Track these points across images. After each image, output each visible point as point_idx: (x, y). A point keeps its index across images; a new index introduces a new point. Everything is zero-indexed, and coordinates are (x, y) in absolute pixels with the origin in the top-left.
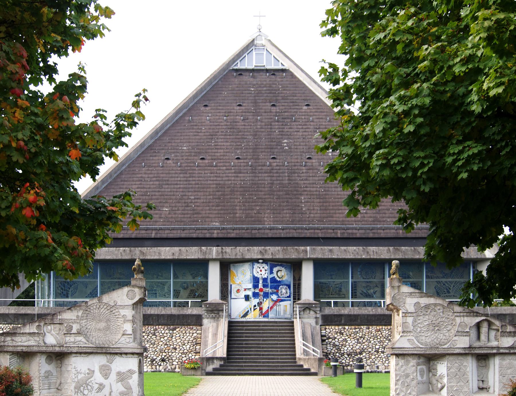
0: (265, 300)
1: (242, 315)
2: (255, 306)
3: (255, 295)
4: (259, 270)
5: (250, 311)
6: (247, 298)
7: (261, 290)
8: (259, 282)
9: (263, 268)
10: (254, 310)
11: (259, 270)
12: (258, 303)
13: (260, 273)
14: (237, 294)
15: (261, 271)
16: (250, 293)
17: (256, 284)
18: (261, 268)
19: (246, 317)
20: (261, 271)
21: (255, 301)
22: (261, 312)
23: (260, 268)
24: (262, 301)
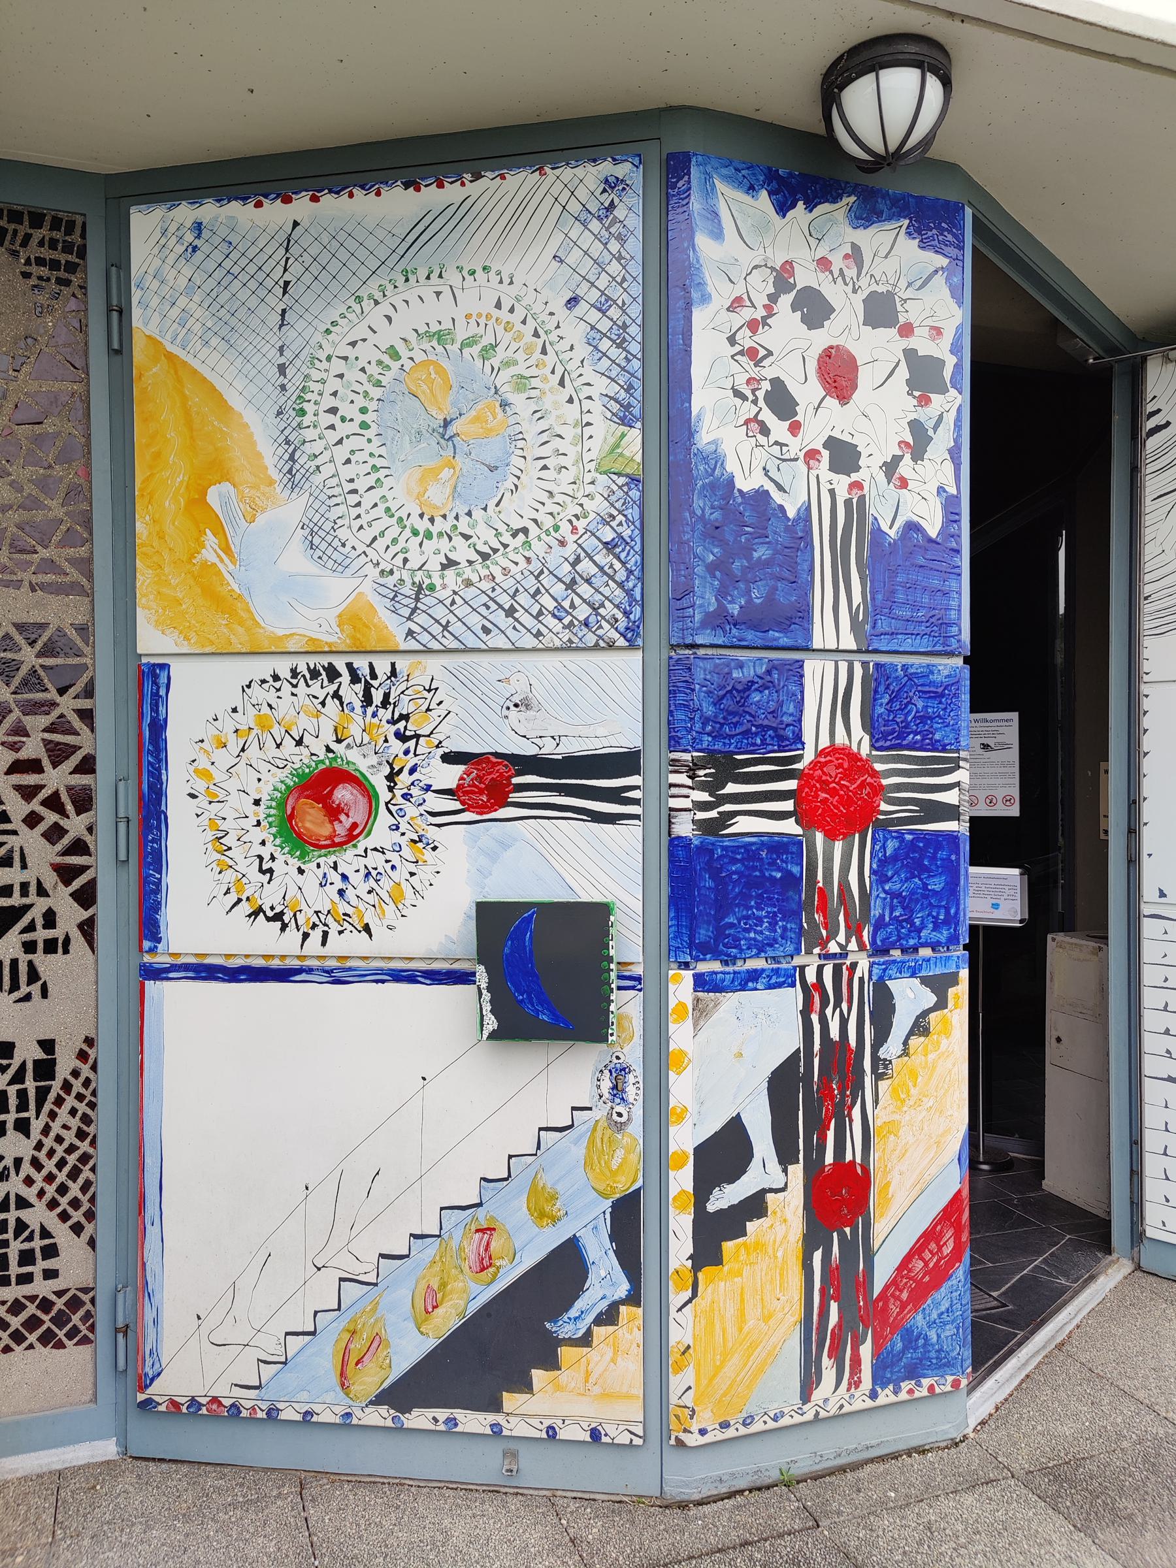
0: (910, 996)
1: (409, 1348)
2: (724, 1153)
3: (724, 904)
4: (792, 348)
5: (605, 1279)
6: (538, 974)
7: (838, 797)
8: (799, 617)
9: (881, 311)
10: (714, 1234)
11: (792, 348)
12: (784, 1084)
13: (823, 419)
14: (303, 884)
15: (838, 374)
16: (602, 865)
17: (751, 662)
18: (845, 327)
19: (523, 1413)
20: (838, 374)
21: (728, 1049)
22: (844, 1280)
23: (814, 309)
24: (844, 1022)
